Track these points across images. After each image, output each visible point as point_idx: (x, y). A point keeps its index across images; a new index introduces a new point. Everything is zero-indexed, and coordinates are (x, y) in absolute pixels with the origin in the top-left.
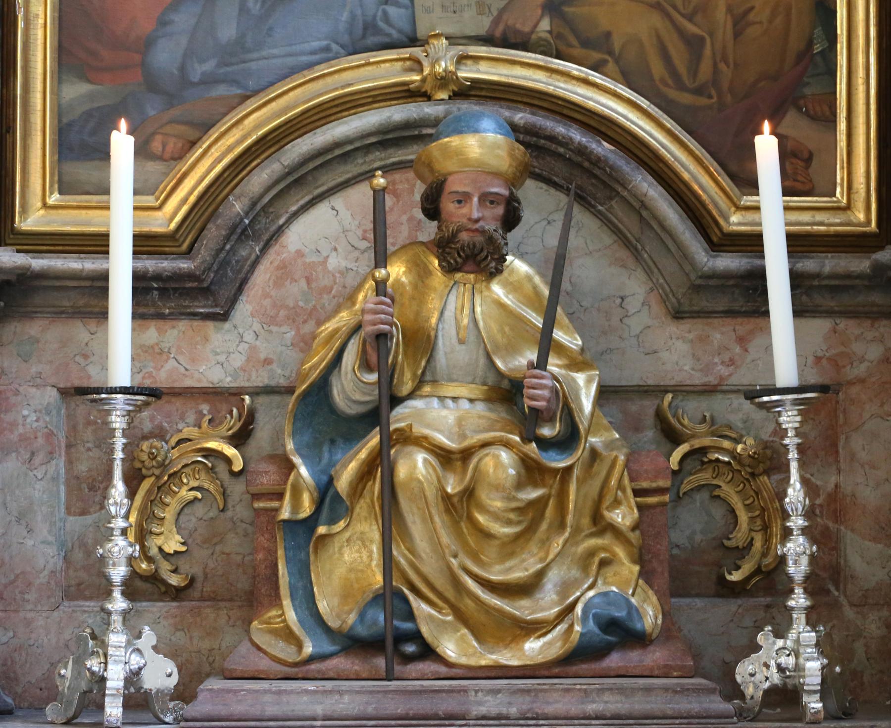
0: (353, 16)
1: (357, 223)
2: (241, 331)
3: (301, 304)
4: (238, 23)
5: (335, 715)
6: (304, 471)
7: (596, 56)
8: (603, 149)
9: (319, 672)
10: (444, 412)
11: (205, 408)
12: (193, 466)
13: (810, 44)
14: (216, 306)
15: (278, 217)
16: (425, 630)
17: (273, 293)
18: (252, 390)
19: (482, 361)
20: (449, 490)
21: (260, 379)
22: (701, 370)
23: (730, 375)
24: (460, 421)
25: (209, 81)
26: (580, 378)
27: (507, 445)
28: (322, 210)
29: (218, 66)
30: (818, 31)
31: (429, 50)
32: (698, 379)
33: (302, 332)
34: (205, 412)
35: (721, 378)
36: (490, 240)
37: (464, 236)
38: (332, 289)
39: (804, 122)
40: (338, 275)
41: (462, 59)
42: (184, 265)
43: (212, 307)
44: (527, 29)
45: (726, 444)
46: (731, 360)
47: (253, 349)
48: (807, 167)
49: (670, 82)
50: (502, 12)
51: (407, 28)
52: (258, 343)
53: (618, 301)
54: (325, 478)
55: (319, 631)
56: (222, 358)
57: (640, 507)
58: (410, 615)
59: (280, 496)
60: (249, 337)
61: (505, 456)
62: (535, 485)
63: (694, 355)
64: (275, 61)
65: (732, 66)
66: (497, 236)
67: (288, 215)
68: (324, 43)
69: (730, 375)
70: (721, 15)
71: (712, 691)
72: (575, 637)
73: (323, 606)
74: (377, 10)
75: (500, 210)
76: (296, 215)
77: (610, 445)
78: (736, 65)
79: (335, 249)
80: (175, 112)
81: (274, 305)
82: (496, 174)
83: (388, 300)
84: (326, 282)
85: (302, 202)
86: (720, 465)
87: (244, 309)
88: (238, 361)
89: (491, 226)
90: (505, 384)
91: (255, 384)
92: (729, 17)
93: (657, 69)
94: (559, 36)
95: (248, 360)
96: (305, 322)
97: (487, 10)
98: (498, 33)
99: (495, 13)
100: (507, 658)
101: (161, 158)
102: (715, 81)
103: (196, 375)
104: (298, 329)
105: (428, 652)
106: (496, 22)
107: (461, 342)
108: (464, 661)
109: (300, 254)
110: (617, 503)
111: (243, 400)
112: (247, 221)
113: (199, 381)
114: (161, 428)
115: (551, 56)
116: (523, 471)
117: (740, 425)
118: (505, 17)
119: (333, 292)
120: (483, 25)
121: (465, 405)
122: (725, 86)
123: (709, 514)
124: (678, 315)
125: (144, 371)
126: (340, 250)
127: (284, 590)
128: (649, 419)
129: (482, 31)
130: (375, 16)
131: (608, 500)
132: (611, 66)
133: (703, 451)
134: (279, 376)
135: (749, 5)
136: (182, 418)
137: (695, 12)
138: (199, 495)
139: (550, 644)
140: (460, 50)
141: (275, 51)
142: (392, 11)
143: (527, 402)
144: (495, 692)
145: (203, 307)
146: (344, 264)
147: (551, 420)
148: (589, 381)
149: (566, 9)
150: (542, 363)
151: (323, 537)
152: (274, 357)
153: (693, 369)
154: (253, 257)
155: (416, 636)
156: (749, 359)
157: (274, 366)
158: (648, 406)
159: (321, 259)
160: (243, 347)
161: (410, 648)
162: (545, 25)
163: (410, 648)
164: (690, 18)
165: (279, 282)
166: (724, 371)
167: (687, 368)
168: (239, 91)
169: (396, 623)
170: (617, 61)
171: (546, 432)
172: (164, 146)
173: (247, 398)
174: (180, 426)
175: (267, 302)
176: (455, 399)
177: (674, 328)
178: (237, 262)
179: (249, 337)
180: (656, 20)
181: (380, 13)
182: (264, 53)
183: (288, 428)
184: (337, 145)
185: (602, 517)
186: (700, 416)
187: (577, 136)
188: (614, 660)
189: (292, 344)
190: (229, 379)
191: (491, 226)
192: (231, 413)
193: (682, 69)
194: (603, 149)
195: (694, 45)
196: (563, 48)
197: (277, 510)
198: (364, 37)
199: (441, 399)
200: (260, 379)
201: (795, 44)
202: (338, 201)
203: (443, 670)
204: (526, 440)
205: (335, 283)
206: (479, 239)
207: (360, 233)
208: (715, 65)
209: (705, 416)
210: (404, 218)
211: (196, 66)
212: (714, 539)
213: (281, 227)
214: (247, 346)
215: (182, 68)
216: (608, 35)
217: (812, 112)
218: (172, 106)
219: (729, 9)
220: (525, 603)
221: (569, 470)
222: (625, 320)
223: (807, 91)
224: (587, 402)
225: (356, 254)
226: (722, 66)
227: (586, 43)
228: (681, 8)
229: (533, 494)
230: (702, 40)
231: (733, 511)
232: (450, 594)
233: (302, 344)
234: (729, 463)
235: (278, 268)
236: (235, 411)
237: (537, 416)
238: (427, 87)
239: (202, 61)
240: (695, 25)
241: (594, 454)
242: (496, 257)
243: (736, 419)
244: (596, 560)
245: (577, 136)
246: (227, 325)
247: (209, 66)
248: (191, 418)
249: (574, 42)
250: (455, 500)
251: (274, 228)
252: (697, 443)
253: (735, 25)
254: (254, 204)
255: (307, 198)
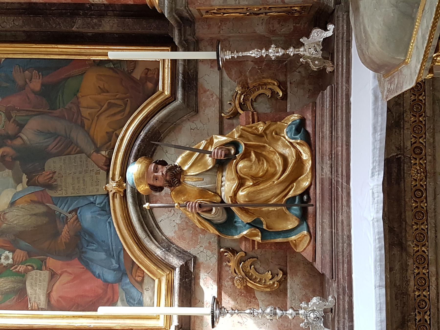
0: (99, 214)
1: (165, 214)
2: (199, 252)
3: (191, 232)
4: (100, 252)
5: (330, 224)
6: (245, 233)
7: (114, 136)
8: (143, 134)
9: (313, 229)
10: (226, 185)
11: (224, 264)
12: (243, 268)
13: (111, 68)
14: (191, 260)
15: (163, 239)
16: (299, 192)
17: (188, 241)
18: (219, 248)
19: (209, 173)
20: (251, 184)
21: (215, 246)
22: (215, 105)
23: (216, 95)
24: (229, 180)
25: (118, 262)
26: (215, 141)
27: (237, 164)
28: (161, 225)
29: (114, 259)
30: (107, 66)
31: (110, 190)
32: (217, 105)
33: (200, 232)
34: (226, 264)
35: (217, 98)
36: (169, 170)
37: (168, 178)
38: (186, 222)
39: (136, 70)
40: (182, 220)
41: (113, 179)
42: (178, 270)
43: (191, 261)
44: (105, 159)
45: (238, 96)
46: (211, 95)
47: (205, 248)
48: (151, 70)
49: (122, 113)
50: (99, 167)
51: (103, 197)
52: (203, 246)
53: (192, 130)
54: (247, 226)
55: (299, 229)
56: (208, 258)
57: (258, 121)
58: (294, 198)
59: (254, 241)
60: (202, 249)
61: (241, 165)
62: (250, 155)
63: (210, 107)
64: (113, 240)
65: (117, 94)
66: (168, 167)
67: (162, 236)
68: (107, 223)
69: (216, 95)
70: (101, 97)
71: (323, 94)
72: (302, 142)
73: (290, 227)
74: (97, 207)
75: (160, 166)
76: (162, 233)
77: (237, 132)
78: (117, 92)
79: (174, 221)
80: (128, 273)
81: (192, 241)
82: (147, 167)
83: (188, 203)
84: (184, 223)
85: (158, 231)
86: (245, 98)
87: (193, 251)
88: (209, 253)
89: (165, 169)
90: (217, 165)
91: (217, 247)
92: (101, 94)
93: (118, 117)
94: (107, 149)
95: (209, 249)
96: (197, 231)
97: (98, 171)
98: (106, 168)
99: (99, 169)
100: (308, 165)
101: (143, 277)
102: (122, 99)
103: (214, 267)
104: (200, 233)
105: (307, 191)
106: (102, 169)
107: (203, 180)
108: (309, 180)
109: (175, 232)
110: (257, 129)
111: (222, 251)
112: (164, 250)
113: (215, 266)
114: (231, 278)
115: (113, 151)
116: (246, 159)
117: (232, 92)
118: (101, 166)
119: (188, 221)
120: (103, 173)
121: (224, 178)
122: (124, 96)
123: (261, 102)
124: (197, 112)
125: (212, 284)
126: (174, 219)
127: (285, 240)
128: (230, 121)
129: (105, 173)
130: (99, 207)
131: (256, 132)
132: (117, 132)
133: (240, 104)
134: (214, 240)
135: (98, 87)
136: (228, 271)
137: (100, 105)
138: (252, 266)
139: (304, 151)
140: (110, 180)
141: (110, 240)
142: (97, 202)
143: (222, 158)
144: (322, 169)
145: (191, 264)
146: (179, 218)
147: (229, 150)
148: (216, 138)
149: (98, 146)
150: (210, 153)
151: (267, 227)
152: (208, 241)
153: (214, 107)
154: (176, 247)
155: (301, 195)
156: (211, 89)
157: (211, 241)
158: (226, 121)
159: (177, 225)
160: (205, 250)
161: (305, 197)
162: (103, 153)
163: (305, 197)
164: (103, 106)
165: (184, 239)
166: (215, 97)
167: (214, 109)
168: (122, 252)
169: (296, 203)
170: (116, 130)
171: (233, 152)
172: (140, 276)
173: (222, 250)
174: (230, 272)
175: (190, 243)
176: (222, 182)
177: (201, 113)
178: (177, 253)
179: (202, 249)
180: (102, 117)
181: (98, 206)
182: (110, 244)
183: (230, 237)
184: (139, 220)
185: (261, 134)
186: (229, 105)
187: (138, 142)
188: (309, 129)
189: (204, 235)
190: (215, 256)
191: (165, 169)
192: (226, 255)
193: (119, 109)
194: (143, 134)
195: (111, 105)
196: (111, 148)
197: (258, 242)
198: (106, 211)
199: (222, 186)
200: (215, 245)
201: (111, 73)
202: (158, 219)
203: (312, 186)
204: (235, 158)
205: (185, 221)
206: (169, 173)
207: (169, 213)
208: (117, 99)
209: (229, 103)
210: (164, 198)
211: (113, 266)
212: (268, 101)
213: (166, 238)
214: (204, 250)
215: (114, 270)
216: (107, 133)
217: (133, 68)
218: (126, 274)
219: (100, 94)
220: (290, 160)
221: (245, 144)
222: (198, 128)
223: (126, 69)
224: (223, 139)
225: (175, 214)
226: (117, 96)
227: (110, 140)
228: (98, 110)
229: (253, 156)
230: (109, 103)
231: (260, 95)
232: (287, 184)
233: (204, 232)
234: (244, 95)
235: (179, 239)
236: (225, 254)
237: (227, 154)
238: (122, 190)
239: (112, 264)
240: (105, 104)
241: (240, 136)
242: (175, 168)
243: (230, 93)
244: (275, 136)
245: (138, 142)
246: (198, 256)
247: (114, 261)
248: (227, 268)
249: (110, 143)
250: (255, 182)
251: (166, 240)
252: (238, 106)
253: (104, 92)
254: (158, 247)
255: (157, 229)
